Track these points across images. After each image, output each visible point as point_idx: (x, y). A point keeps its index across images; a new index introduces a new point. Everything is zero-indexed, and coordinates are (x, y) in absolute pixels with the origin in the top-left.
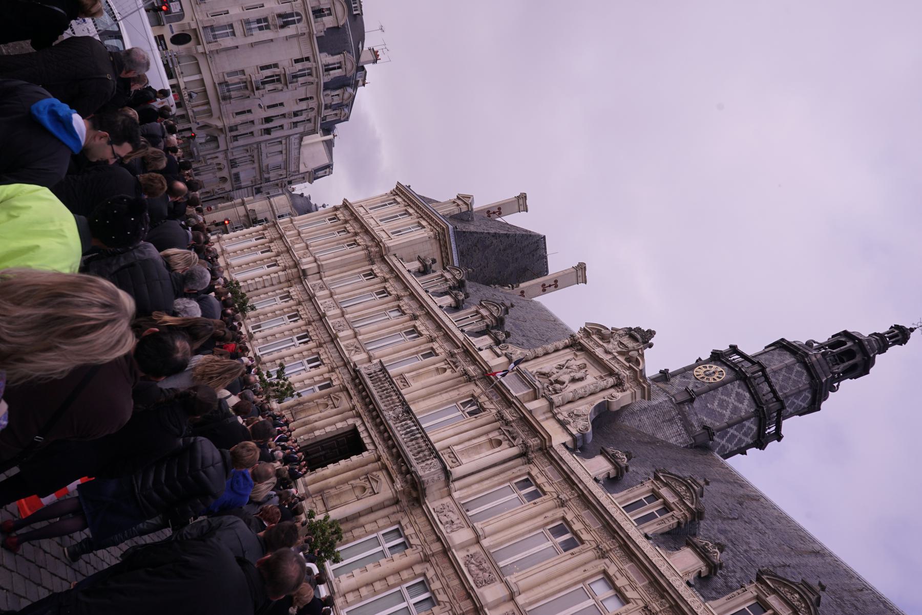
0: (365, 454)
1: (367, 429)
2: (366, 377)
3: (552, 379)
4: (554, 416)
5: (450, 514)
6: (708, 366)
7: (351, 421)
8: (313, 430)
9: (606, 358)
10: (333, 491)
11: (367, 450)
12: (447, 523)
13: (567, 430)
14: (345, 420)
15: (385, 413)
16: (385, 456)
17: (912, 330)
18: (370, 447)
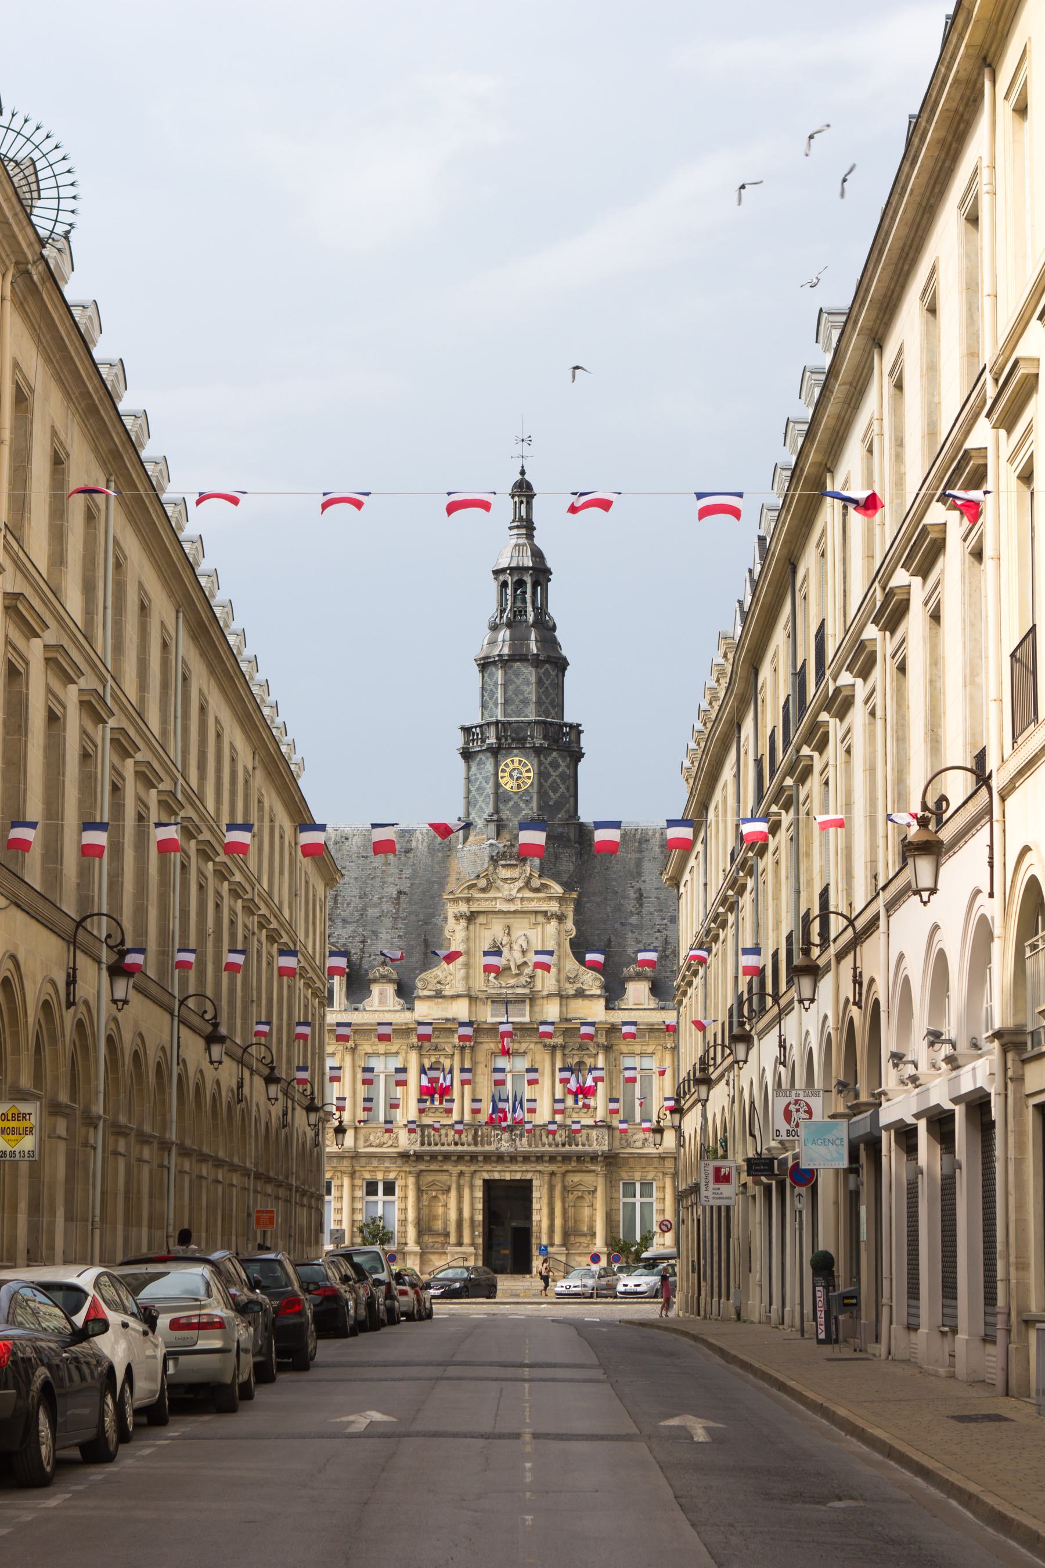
0: (535, 1183)
1: (499, 1172)
2: (426, 1148)
3: (514, 971)
4: (568, 997)
5: (635, 1137)
6: (502, 767)
7: (479, 1183)
8: (472, 1220)
9: (516, 906)
10: (571, 1223)
11: (531, 1181)
12: (643, 1144)
13: (592, 996)
14: (472, 1187)
15: (503, 1149)
16: (553, 1167)
17: (523, 473)
18: (529, 1176)
